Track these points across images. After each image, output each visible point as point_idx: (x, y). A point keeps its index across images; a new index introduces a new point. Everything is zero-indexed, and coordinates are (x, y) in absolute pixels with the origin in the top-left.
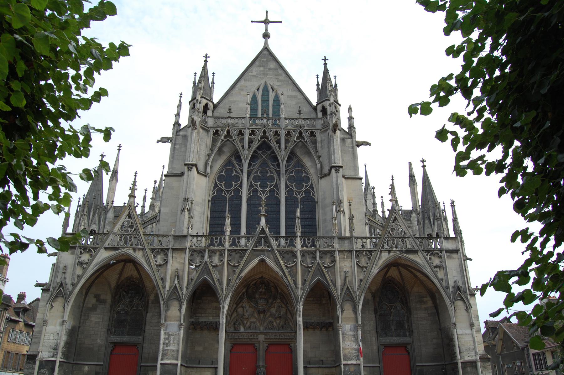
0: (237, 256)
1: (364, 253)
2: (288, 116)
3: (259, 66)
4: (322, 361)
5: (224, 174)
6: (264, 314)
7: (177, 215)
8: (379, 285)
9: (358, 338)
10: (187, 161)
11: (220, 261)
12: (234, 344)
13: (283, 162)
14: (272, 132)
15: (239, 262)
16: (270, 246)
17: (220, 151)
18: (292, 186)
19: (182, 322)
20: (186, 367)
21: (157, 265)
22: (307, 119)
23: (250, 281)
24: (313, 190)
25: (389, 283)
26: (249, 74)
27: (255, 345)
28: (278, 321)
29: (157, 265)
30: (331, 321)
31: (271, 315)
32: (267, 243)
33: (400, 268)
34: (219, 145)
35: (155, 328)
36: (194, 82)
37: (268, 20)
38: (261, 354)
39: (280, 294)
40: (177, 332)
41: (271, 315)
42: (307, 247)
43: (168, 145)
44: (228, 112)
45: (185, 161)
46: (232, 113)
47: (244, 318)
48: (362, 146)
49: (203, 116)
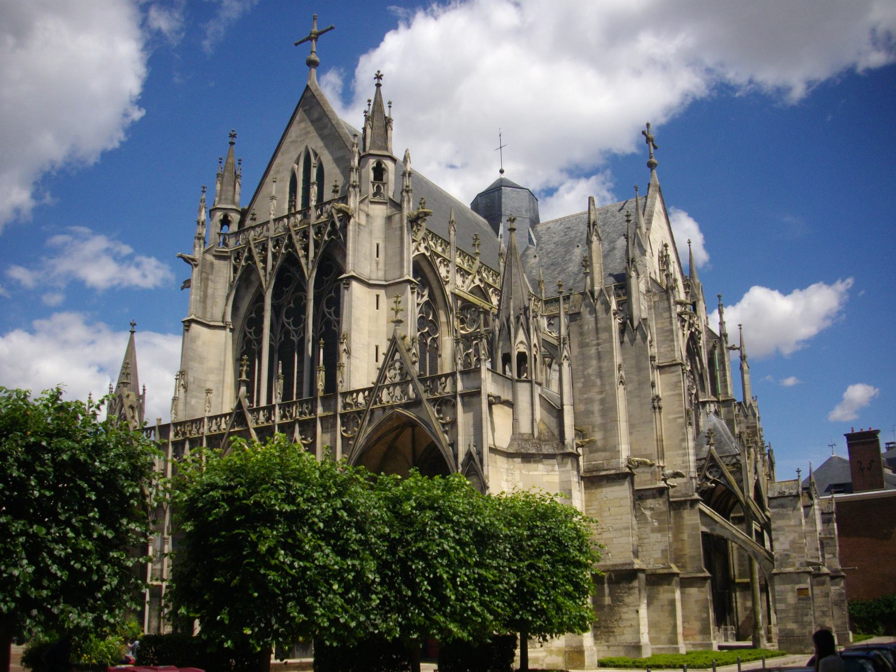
3: (300, 122)
26: (288, 140)
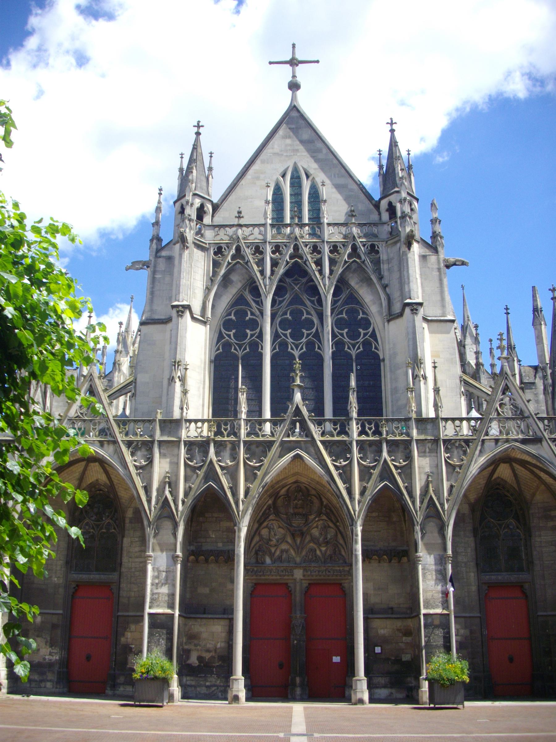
0: (258, 450)
1: (457, 444)
2: (334, 220)
4: (392, 608)
5: (233, 317)
6: (302, 537)
7: (162, 385)
8: (481, 491)
9: (446, 575)
10: (176, 300)
11: (232, 459)
12: (256, 584)
13: (326, 297)
14: (308, 247)
15: (262, 461)
16: (309, 434)
17: (226, 281)
18: (342, 335)
19: (179, 553)
20: (185, 618)
21: (136, 466)
22: (365, 224)
23: (278, 488)
24: (376, 340)
25: (497, 489)
27: (289, 585)
28: (324, 549)
29: (136, 466)
30: (405, 548)
31: (314, 540)
32: (305, 428)
33: (514, 464)
34: (223, 271)
35: (137, 560)
36: (181, 170)
37: (296, 60)
38: (298, 599)
39: (325, 507)
40: (172, 568)
41: (314, 540)
42: (367, 435)
43: (145, 274)
44: (236, 217)
45: (170, 299)
46: (243, 217)
47: (271, 546)
48: (454, 266)
49: (197, 224)
